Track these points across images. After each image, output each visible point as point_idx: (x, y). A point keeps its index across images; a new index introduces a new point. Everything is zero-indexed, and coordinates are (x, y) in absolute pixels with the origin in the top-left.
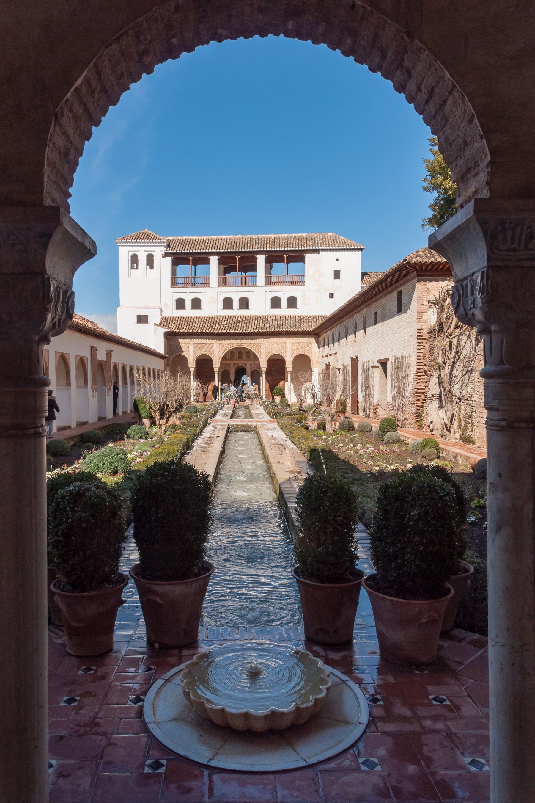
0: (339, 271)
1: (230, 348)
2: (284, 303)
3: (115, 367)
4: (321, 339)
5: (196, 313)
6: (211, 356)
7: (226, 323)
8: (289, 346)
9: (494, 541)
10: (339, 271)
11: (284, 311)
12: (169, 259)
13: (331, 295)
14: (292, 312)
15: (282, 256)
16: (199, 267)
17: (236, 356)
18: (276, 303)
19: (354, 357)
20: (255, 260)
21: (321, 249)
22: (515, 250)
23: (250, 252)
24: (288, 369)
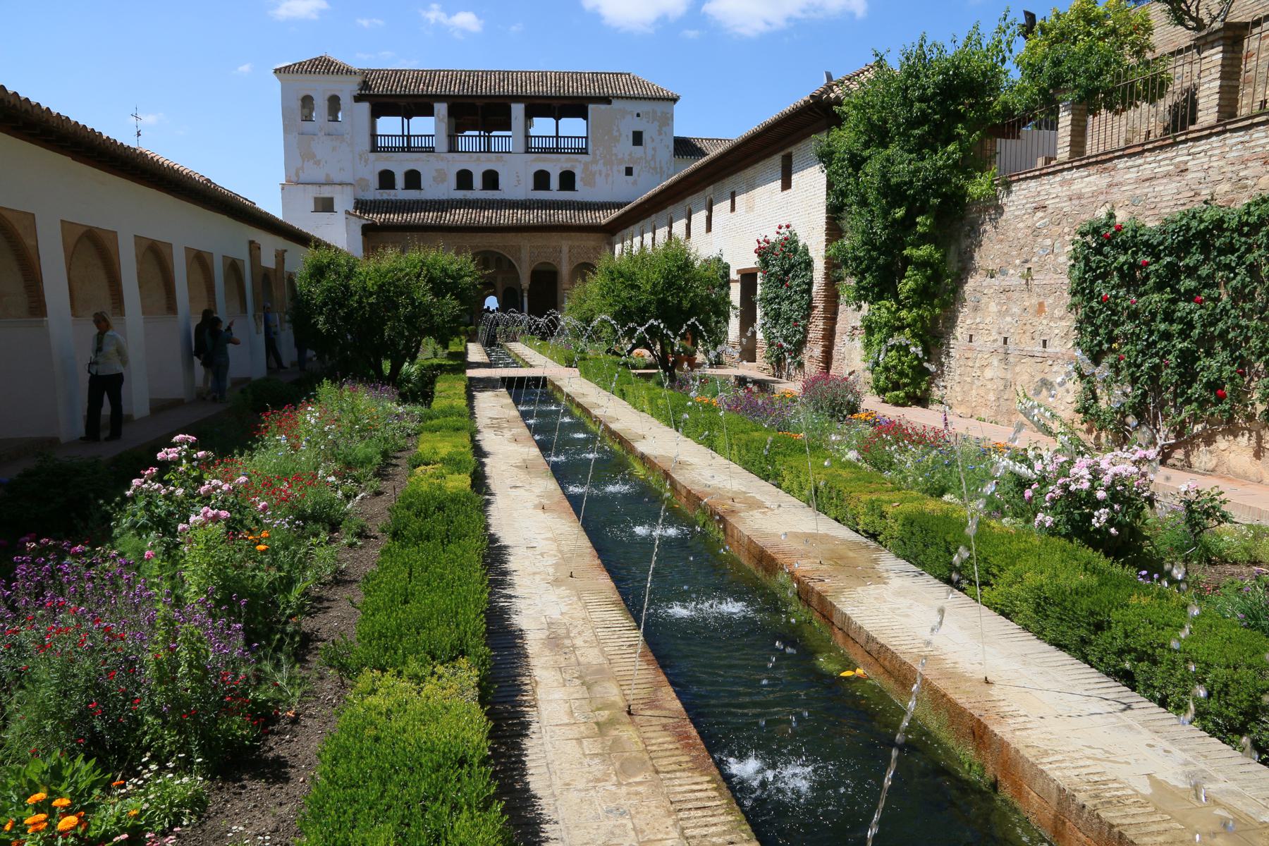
5: (412, 195)
8: (565, 249)
12: (365, 107)
13: (629, 171)
15: (549, 105)
16: (415, 121)
18: (541, 180)
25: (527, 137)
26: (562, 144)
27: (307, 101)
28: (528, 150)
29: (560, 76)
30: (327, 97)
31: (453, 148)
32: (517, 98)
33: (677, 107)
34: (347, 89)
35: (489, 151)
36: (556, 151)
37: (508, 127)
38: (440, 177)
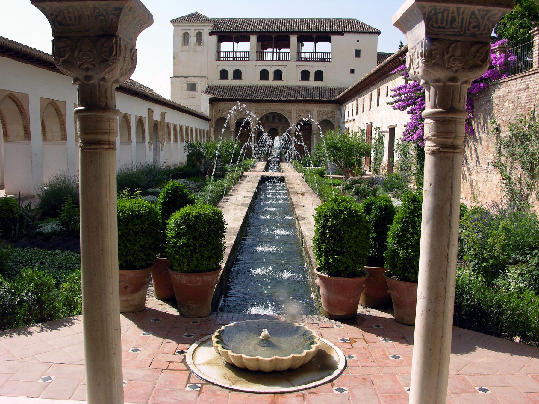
1: (265, 113)
2: (312, 76)
3: (168, 126)
5: (237, 83)
7: (262, 91)
8: (315, 112)
9: (424, 230)
11: (312, 83)
12: (215, 38)
13: (352, 71)
14: (318, 84)
16: (240, 43)
17: (270, 120)
18: (305, 75)
19: (369, 124)
20: (288, 39)
21: (345, 32)
22: (444, 28)
23: (284, 32)
24: (314, 132)
27: (186, 35)
28: (300, 59)
29: (317, 21)
31: (260, 58)
32: (293, 33)
33: (380, 37)
34: (206, 29)
35: (280, 60)
36: (315, 60)
37: (288, 47)
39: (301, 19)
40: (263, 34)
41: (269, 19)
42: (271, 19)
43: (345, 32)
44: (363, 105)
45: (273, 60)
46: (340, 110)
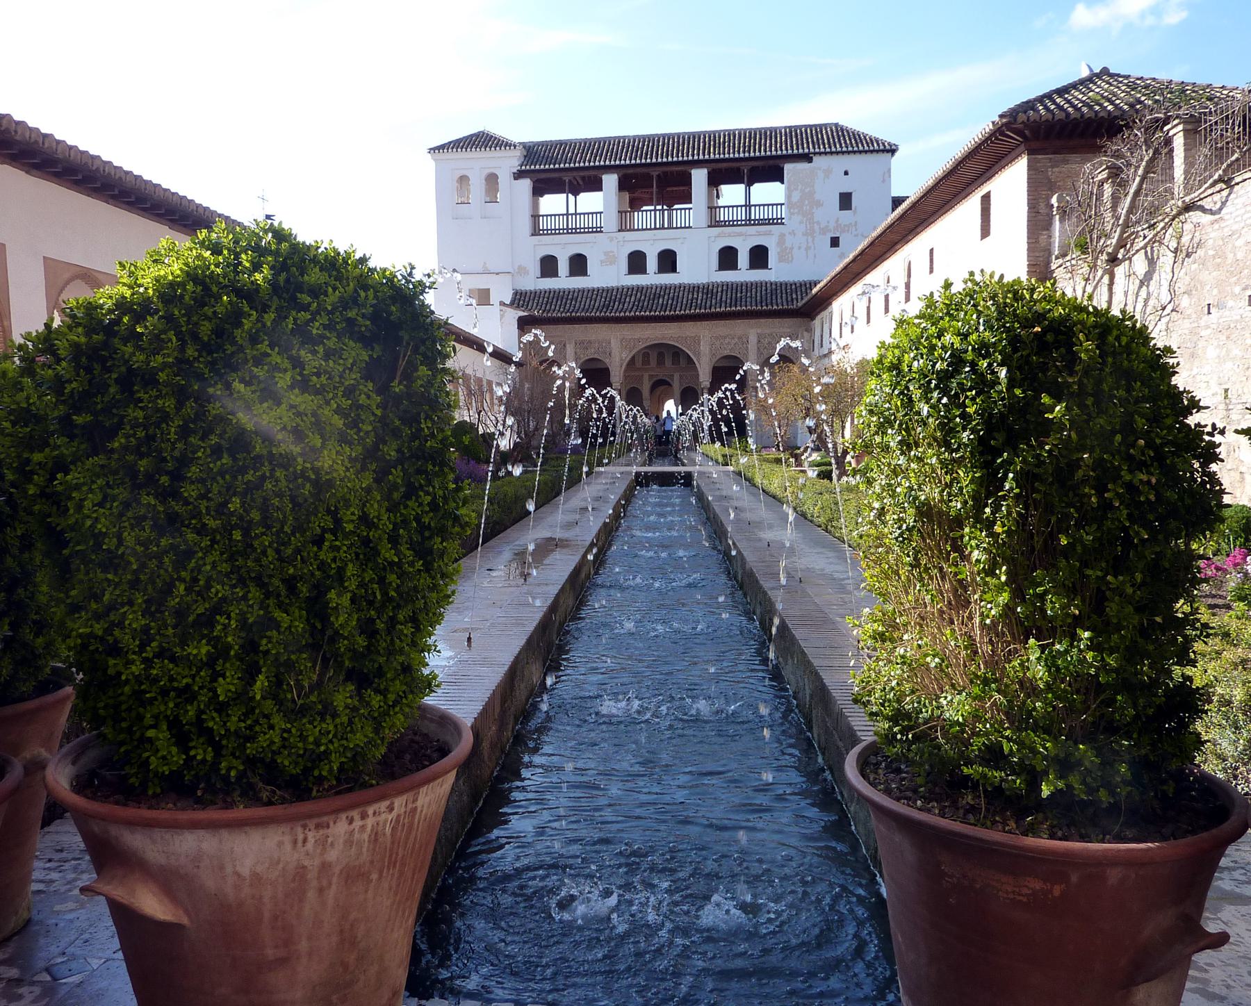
0: (850, 194)
1: (641, 346)
2: (743, 259)
4: (817, 322)
5: (578, 283)
6: (607, 361)
8: (753, 339)
10: (850, 194)
13: (835, 242)
15: (738, 169)
16: (583, 197)
17: (653, 362)
18: (728, 258)
20: (687, 181)
21: (815, 154)
23: (678, 163)
25: (712, 209)
26: (756, 214)
27: (463, 180)
28: (715, 223)
30: (483, 177)
33: (896, 160)
36: (749, 222)
37: (687, 198)
38: (610, 259)
39: (714, 132)
40: (631, 171)
41: (644, 137)
42: (649, 137)
43: (815, 154)
44: (868, 308)
45: (655, 228)
46: (810, 330)
